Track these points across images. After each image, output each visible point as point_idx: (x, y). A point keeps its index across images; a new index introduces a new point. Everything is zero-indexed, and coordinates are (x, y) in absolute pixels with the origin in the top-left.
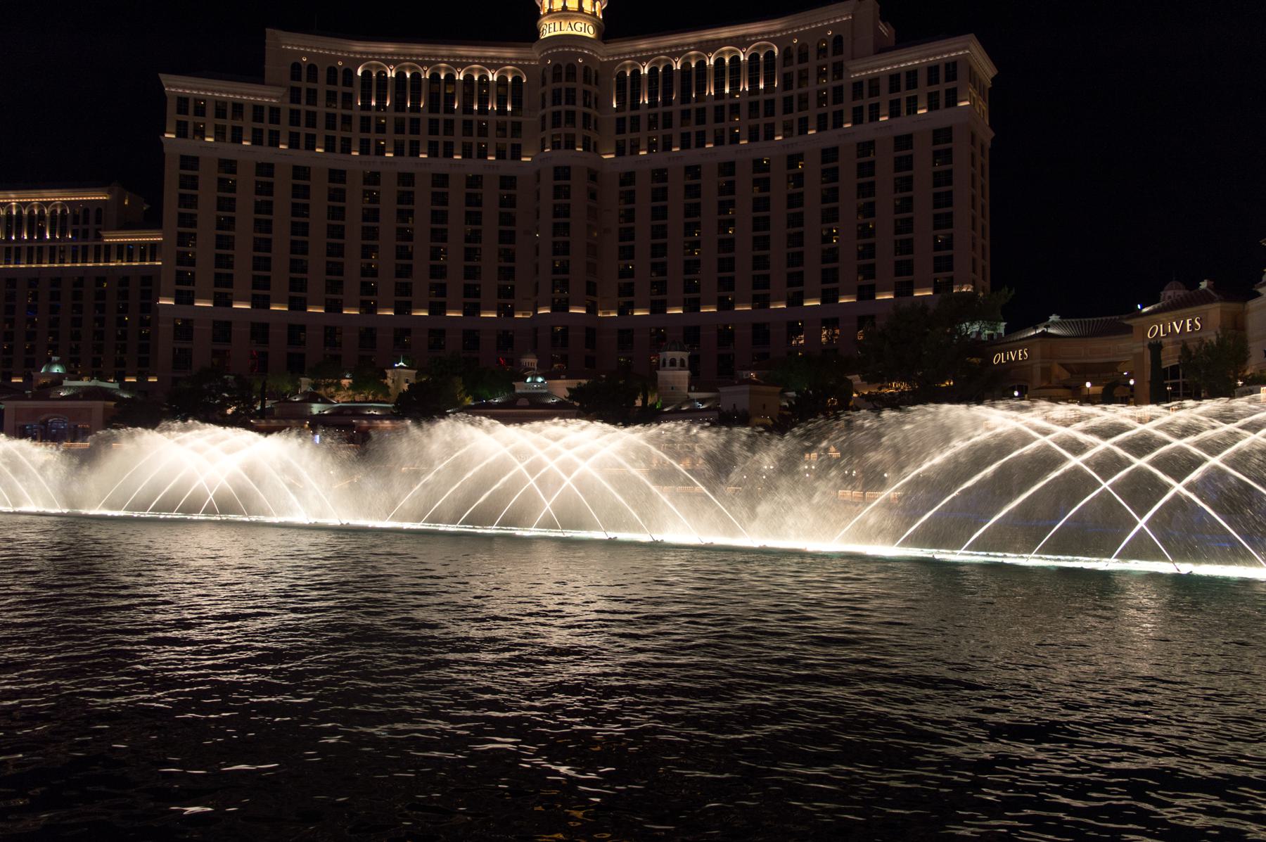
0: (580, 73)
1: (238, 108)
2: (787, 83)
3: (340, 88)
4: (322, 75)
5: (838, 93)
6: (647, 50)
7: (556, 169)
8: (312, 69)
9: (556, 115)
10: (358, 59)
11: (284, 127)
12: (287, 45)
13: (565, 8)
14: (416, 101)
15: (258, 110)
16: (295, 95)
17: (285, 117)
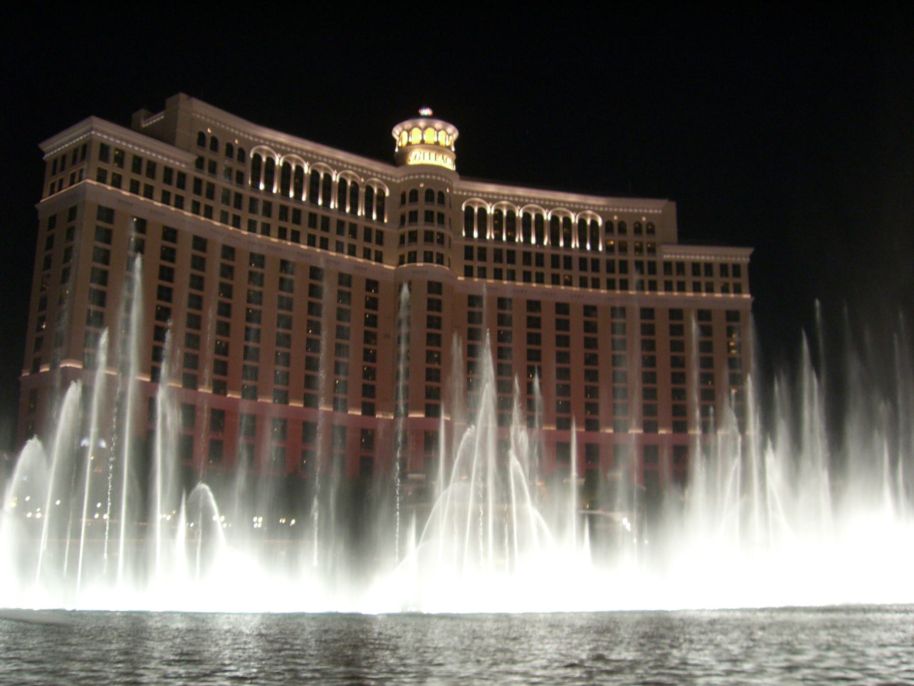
0: (447, 200)
1: (152, 167)
2: (609, 249)
3: (236, 166)
4: (222, 148)
5: (652, 268)
6: (493, 194)
7: (430, 284)
8: (215, 142)
9: (429, 237)
10: (249, 141)
11: (189, 196)
12: (196, 112)
13: (437, 143)
14: (298, 193)
15: (168, 171)
16: (200, 163)
17: (190, 184)
